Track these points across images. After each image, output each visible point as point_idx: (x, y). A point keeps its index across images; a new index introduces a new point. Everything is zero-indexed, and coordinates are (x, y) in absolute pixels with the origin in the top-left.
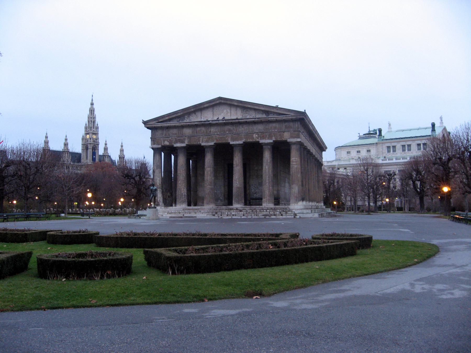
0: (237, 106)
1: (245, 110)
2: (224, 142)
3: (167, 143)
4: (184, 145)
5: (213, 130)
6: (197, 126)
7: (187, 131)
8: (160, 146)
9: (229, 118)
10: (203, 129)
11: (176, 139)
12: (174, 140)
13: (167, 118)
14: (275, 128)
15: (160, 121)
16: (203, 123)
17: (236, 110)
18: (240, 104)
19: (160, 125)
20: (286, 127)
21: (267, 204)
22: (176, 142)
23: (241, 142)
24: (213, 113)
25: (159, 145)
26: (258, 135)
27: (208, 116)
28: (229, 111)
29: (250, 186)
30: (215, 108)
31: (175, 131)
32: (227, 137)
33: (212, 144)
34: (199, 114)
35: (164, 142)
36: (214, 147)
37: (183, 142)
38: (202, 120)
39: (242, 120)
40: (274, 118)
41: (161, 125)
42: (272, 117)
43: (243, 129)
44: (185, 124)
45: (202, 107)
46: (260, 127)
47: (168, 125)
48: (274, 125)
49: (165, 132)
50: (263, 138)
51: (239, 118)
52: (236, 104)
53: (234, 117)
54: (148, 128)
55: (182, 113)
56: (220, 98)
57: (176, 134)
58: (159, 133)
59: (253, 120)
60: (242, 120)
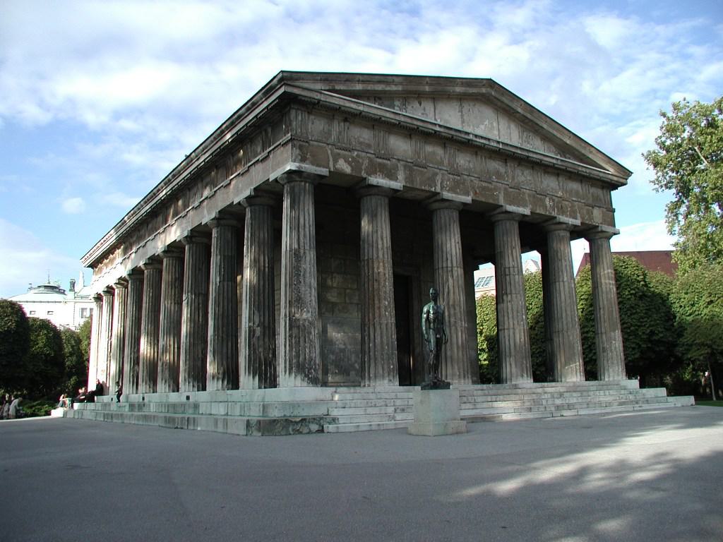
1: (525, 134)
2: (491, 201)
4: (397, 185)
5: (464, 160)
7: (401, 146)
8: (324, 171)
12: (366, 162)
13: (359, 87)
15: (338, 87)
16: (453, 133)
19: (337, 100)
21: (573, 375)
22: (374, 169)
24: (462, 116)
25: (318, 165)
26: (553, 200)
28: (495, 124)
30: (466, 106)
31: (364, 135)
32: (495, 189)
33: (468, 199)
34: (428, 105)
35: (335, 161)
37: (391, 175)
39: (535, 156)
40: (588, 171)
41: (341, 103)
44: (409, 121)
47: (361, 108)
50: (562, 210)
56: (490, 83)
57: (369, 146)
60: (535, 156)
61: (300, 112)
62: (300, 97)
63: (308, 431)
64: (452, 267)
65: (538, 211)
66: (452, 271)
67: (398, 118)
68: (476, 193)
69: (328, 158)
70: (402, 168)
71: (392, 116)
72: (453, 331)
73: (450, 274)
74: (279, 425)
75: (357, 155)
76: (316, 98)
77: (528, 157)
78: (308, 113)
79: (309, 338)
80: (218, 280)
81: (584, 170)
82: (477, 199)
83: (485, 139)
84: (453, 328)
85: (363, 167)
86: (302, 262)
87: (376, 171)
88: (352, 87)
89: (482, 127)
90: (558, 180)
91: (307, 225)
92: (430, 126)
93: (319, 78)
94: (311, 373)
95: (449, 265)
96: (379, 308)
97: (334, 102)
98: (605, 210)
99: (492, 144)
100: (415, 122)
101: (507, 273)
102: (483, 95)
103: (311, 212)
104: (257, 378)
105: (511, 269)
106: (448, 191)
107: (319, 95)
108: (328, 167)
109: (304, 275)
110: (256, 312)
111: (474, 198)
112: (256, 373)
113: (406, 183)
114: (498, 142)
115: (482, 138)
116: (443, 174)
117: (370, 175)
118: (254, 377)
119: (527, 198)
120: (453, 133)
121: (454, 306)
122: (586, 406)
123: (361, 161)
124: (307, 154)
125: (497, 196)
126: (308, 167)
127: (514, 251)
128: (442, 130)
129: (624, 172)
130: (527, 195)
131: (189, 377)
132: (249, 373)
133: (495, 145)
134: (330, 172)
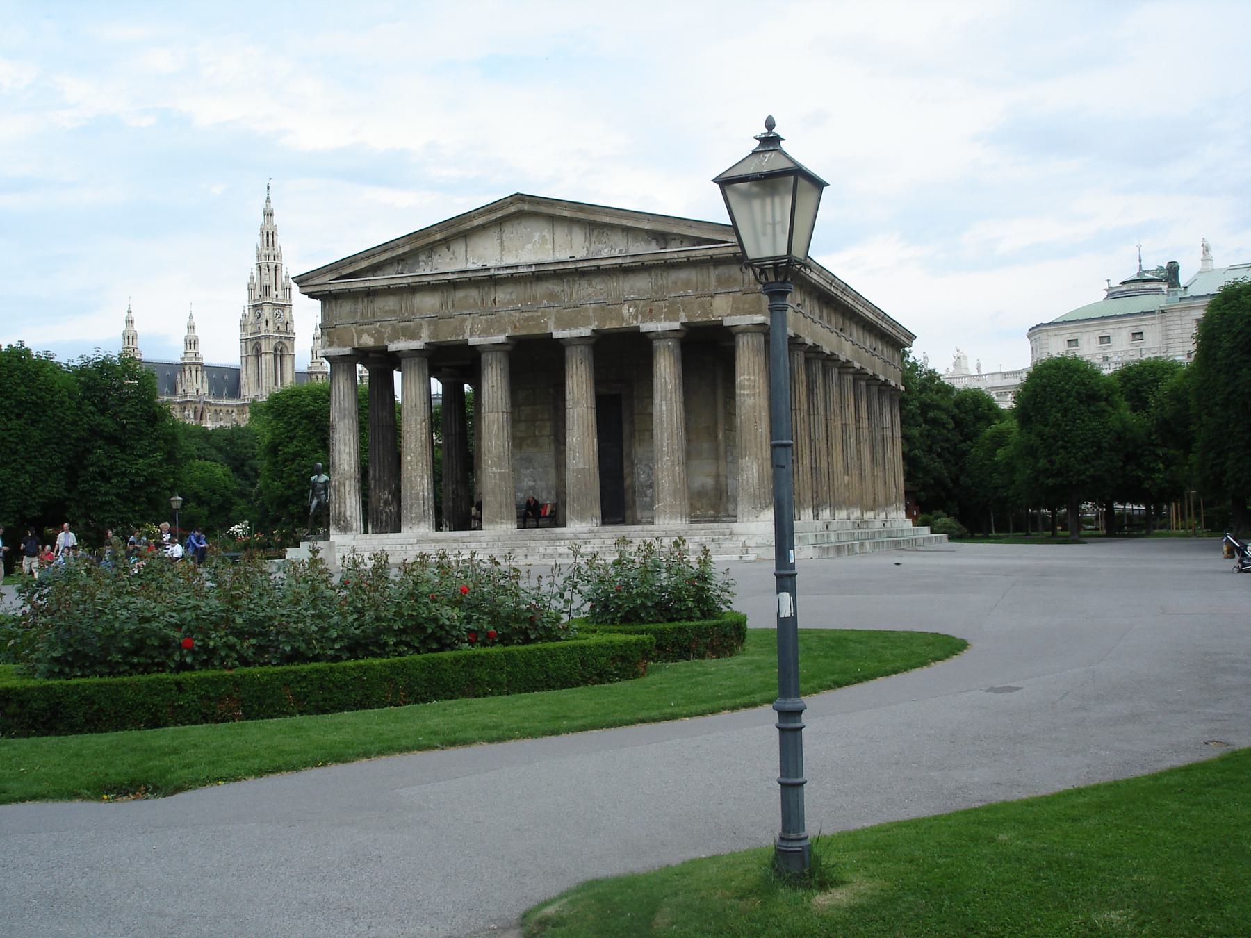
0: (571, 221)
1: (595, 233)
2: (536, 332)
3: (368, 341)
5: (502, 295)
6: (453, 285)
7: (428, 303)
8: (347, 351)
9: (550, 259)
10: (473, 294)
12: (389, 330)
13: (364, 264)
14: (687, 284)
15: (344, 273)
16: (470, 275)
17: (570, 233)
18: (580, 215)
19: (344, 285)
20: (719, 281)
22: (394, 337)
23: (585, 331)
26: (636, 306)
27: (487, 254)
28: (548, 236)
29: (633, 464)
30: (508, 229)
31: (391, 303)
32: (543, 316)
34: (459, 248)
35: (359, 337)
36: (508, 348)
37: (414, 336)
38: (471, 266)
39: (586, 264)
40: (682, 255)
42: (676, 251)
43: (590, 290)
44: (417, 279)
45: (467, 226)
46: (641, 284)
47: (367, 284)
48: (683, 275)
49: (360, 306)
50: (651, 316)
51: (578, 257)
52: (566, 213)
53: (564, 256)
54: (311, 295)
55: (407, 249)
56: (519, 198)
57: (394, 312)
58: (344, 309)
59: (620, 261)
60: (586, 264)
67: (405, 281)
71: (399, 281)
77: (576, 269)
83: (512, 267)
89: (530, 246)
92: (441, 277)
98: (739, 294)
99: (521, 270)
100: (424, 279)
108: (352, 345)
114: (530, 266)
117: (392, 341)
120: (470, 275)
125: (546, 323)
128: (455, 276)
133: (526, 270)
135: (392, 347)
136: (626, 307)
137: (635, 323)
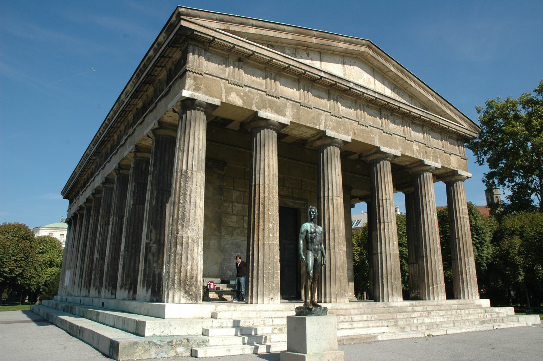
2: (368, 142)
3: (236, 100)
4: (285, 120)
11: (261, 96)
12: (257, 98)
25: (211, 96)
26: (419, 146)
33: (349, 139)
37: (280, 111)
40: (447, 124)
47: (254, 49)
61: (197, 48)
62: (195, 33)
63: (174, 354)
64: (333, 196)
65: (407, 154)
66: (333, 199)
68: (355, 134)
69: (221, 90)
70: (290, 106)
72: (332, 254)
73: (330, 202)
74: (140, 348)
75: (249, 91)
76: (211, 35)
78: (205, 50)
79: (192, 255)
80: (132, 203)
81: (444, 122)
82: (356, 139)
83: (364, 88)
84: (332, 251)
85: (254, 102)
86: (190, 183)
87: (266, 105)
88: (246, 30)
90: (422, 129)
91: (196, 148)
93: (215, 17)
94: (191, 290)
95: (330, 194)
96: (264, 230)
97: (227, 40)
99: (370, 93)
101: (381, 204)
102: (361, 54)
103: (201, 137)
104: (150, 291)
105: (384, 201)
106: (331, 130)
107: (214, 32)
108: (220, 98)
109: (190, 195)
110: (153, 230)
111: (353, 138)
112: (149, 287)
113: (293, 119)
114: (375, 92)
115: (361, 86)
116: (326, 115)
118: (147, 290)
119: (398, 142)
121: (334, 230)
122: (452, 325)
123: (252, 96)
124: (201, 85)
125: (373, 138)
126: (201, 97)
127: (387, 185)
129: (475, 128)
130: (398, 140)
131: (109, 286)
132: (144, 286)
133: (372, 94)
134: (222, 103)
135: (263, 114)
136: (414, 144)
137: (420, 157)
